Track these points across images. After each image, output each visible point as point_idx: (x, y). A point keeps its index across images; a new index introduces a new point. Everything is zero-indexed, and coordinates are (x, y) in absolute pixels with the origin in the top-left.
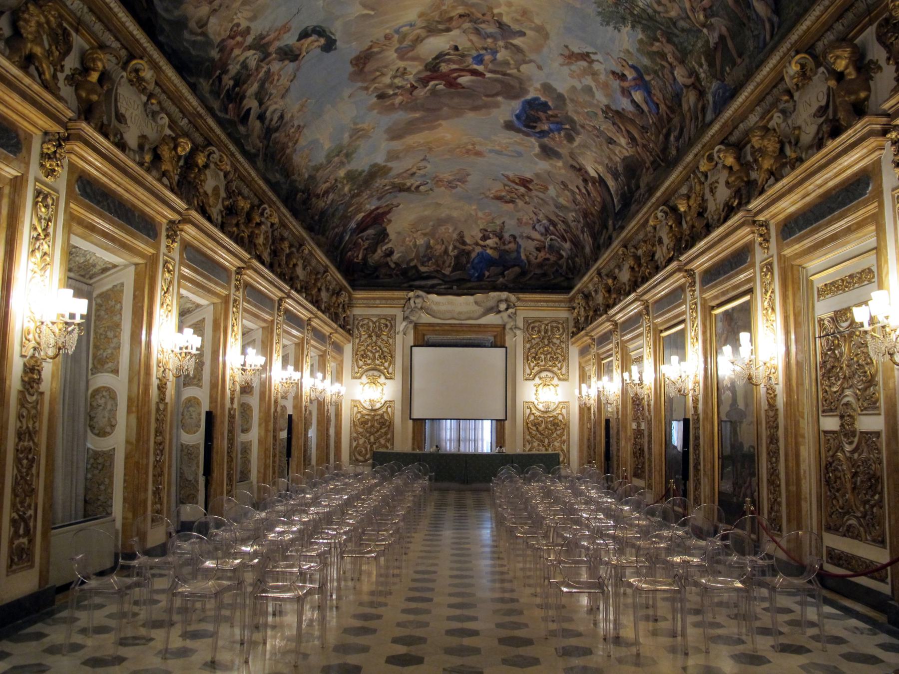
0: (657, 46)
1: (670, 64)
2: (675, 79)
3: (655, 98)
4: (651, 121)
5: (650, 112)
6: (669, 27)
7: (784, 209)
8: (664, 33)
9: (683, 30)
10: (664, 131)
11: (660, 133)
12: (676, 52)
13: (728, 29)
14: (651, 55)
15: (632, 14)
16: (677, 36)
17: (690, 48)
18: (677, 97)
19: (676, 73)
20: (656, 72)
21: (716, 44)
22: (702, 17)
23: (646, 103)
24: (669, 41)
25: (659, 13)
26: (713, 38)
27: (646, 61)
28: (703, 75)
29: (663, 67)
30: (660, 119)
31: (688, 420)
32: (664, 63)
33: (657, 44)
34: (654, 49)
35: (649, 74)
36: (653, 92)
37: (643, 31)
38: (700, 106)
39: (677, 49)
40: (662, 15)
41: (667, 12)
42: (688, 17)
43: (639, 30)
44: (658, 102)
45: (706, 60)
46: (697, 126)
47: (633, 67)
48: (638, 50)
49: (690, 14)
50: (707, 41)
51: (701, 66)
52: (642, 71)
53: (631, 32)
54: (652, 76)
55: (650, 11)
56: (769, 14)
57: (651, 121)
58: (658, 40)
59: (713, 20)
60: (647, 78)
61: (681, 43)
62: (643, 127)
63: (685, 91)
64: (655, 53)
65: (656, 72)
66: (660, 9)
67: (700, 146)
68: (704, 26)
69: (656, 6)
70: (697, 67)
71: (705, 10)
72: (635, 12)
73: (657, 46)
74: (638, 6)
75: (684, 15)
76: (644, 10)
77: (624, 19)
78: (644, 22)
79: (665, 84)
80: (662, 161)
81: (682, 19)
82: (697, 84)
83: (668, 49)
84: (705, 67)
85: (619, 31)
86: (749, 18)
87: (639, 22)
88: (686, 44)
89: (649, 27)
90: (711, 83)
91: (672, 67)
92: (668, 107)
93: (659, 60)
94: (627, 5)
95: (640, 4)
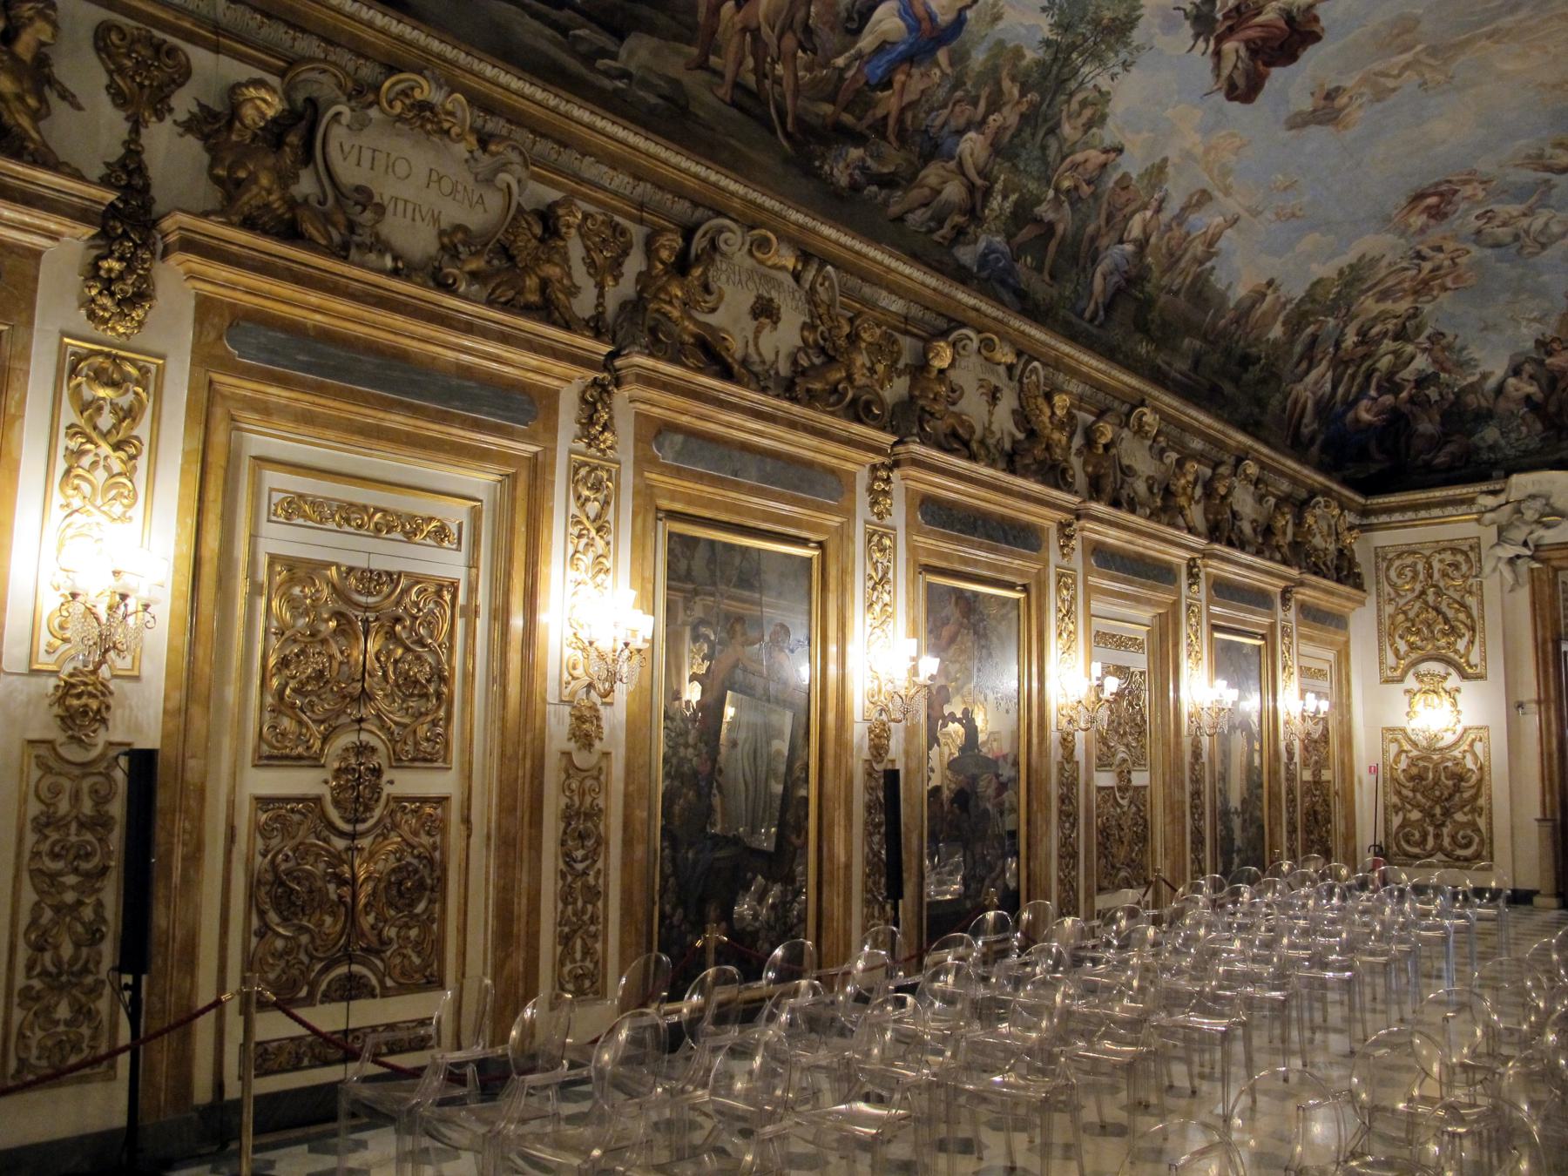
0: (1011, 89)
1: (984, 121)
2: (960, 133)
3: (899, 78)
4: (840, 61)
5: (859, 55)
6: (1045, 121)
7: (1106, 535)
8: (1034, 107)
9: (1044, 148)
10: (847, 118)
11: (833, 101)
12: (1008, 134)
13: (1063, 237)
14: (991, 74)
15: (1073, 47)
16: (1033, 135)
17: (1022, 167)
18: (933, 150)
19: (972, 135)
20: (958, 84)
21: (1041, 221)
22: (1066, 184)
23: (882, 47)
24: (1023, 117)
25: (1068, 102)
26: (1045, 211)
27: (978, 58)
28: (996, 202)
29: (975, 104)
30: (861, 100)
31: (896, 772)
32: (982, 104)
33: (1016, 92)
34: (1006, 84)
35: (952, 64)
36: (916, 72)
37: (1039, 63)
38: (959, 219)
39: (1013, 136)
40: (1065, 107)
41: (1069, 117)
42: (1063, 159)
43: (1041, 54)
44: (897, 86)
45: (1016, 204)
46: (931, 231)
47: (959, 22)
48: (1000, 44)
49: (1068, 160)
50: (1039, 202)
51: (1005, 197)
52: (954, 44)
53: (1039, 38)
54: (949, 71)
55: (1073, 85)
56: (1100, 300)
57: (840, 61)
58: (1023, 94)
59: (1066, 205)
60: (942, 55)
61: (1023, 146)
62: (807, 30)
63: (952, 164)
64: (998, 83)
65: (958, 84)
66: (1074, 105)
67: (1000, 315)
68: (1057, 190)
69: (1079, 97)
70: (999, 186)
71: (1076, 188)
72: (1074, 56)
73: (1011, 89)
74: (1084, 63)
75: (1065, 149)
76: (1076, 72)
77: (1064, 26)
78: (1055, 69)
79: (944, 106)
80: (788, 135)
81: (1060, 148)
82: (978, 196)
83: (1008, 117)
84: (1008, 205)
85: (1044, 9)
86: (1084, 269)
87: (1055, 59)
88: (1024, 155)
89: (1045, 78)
90: (998, 232)
91: (980, 125)
92: (900, 120)
93: (984, 93)
94: (1091, 42)
95: (1085, 70)
